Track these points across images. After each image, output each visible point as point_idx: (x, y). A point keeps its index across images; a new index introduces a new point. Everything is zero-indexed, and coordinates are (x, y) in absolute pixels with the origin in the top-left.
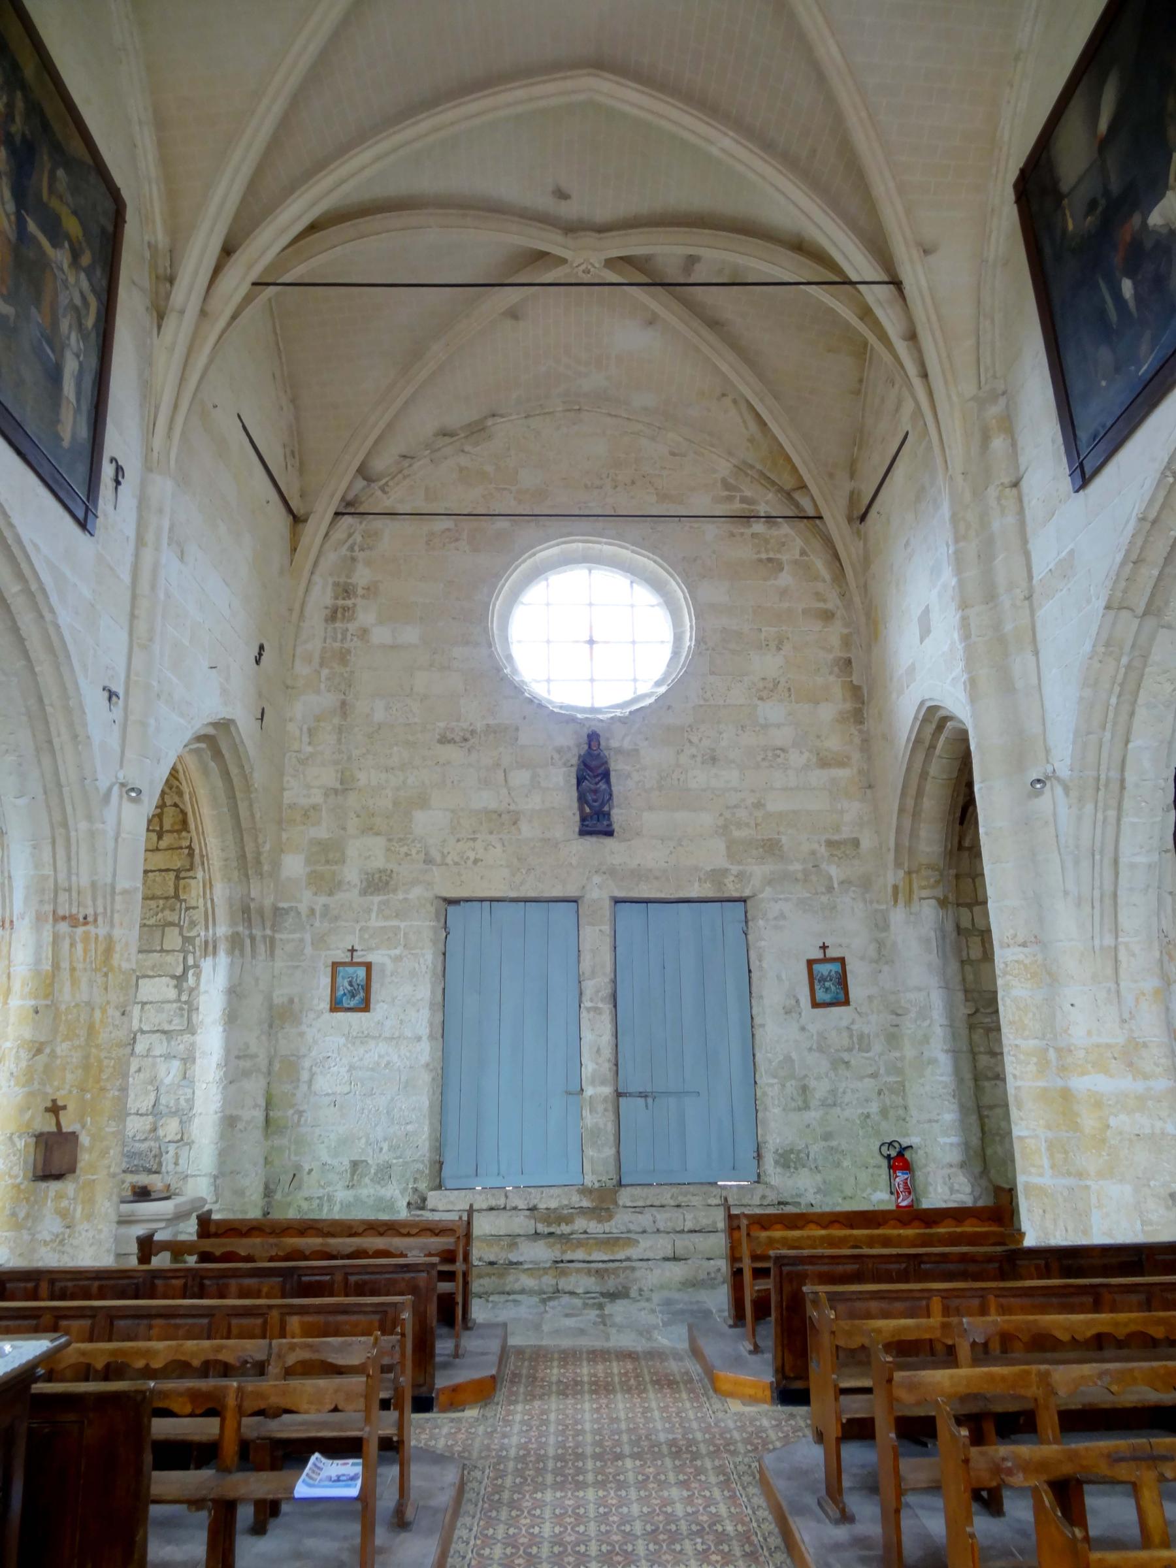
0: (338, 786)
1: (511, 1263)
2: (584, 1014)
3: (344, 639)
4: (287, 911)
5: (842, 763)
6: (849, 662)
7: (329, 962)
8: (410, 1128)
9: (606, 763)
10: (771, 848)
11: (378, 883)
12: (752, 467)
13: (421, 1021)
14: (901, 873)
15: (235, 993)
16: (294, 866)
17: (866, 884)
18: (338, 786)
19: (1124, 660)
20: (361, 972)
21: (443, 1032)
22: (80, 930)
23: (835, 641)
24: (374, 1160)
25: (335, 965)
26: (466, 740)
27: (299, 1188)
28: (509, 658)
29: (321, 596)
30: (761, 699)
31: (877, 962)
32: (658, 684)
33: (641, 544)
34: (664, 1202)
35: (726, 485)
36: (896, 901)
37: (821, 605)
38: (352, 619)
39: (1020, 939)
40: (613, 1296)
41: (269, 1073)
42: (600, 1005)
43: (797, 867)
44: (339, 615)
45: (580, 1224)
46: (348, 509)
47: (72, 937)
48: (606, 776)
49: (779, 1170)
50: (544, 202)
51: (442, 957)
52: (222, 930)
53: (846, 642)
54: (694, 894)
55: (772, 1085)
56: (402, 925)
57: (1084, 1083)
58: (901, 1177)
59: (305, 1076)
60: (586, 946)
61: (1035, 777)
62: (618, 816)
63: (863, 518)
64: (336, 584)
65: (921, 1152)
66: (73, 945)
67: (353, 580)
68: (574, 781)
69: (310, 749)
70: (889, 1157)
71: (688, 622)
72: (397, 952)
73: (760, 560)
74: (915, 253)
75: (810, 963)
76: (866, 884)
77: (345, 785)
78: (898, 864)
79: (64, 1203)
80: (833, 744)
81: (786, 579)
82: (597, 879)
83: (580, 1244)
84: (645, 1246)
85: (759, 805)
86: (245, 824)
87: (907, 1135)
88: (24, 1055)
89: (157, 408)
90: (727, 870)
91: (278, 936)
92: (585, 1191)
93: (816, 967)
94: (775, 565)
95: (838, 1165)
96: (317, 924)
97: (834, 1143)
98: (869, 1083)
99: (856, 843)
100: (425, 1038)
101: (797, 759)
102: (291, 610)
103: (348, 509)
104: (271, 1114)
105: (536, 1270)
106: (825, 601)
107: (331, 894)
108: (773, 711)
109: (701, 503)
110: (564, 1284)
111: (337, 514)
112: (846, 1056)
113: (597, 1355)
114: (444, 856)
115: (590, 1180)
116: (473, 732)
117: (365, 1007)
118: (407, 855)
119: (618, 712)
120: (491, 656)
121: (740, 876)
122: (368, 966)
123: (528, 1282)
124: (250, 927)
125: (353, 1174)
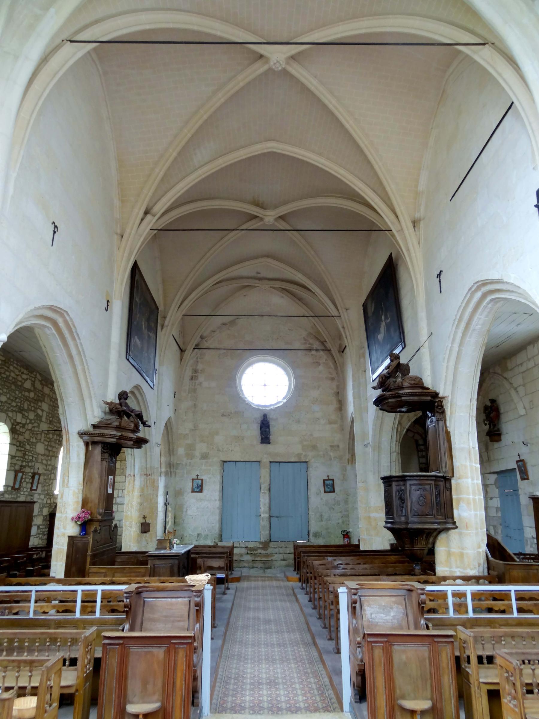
0: (193, 428)
1: (241, 561)
2: (261, 494)
3: (195, 385)
4: (179, 464)
5: (335, 422)
6: (338, 393)
7: (191, 479)
8: (213, 525)
9: (269, 423)
10: (314, 447)
11: (205, 456)
12: (312, 334)
13: (217, 495)
14: (350, 456)
15: (166, 487)
16: (181, 451)
17: (341, 458)
18: (193, 428)
19: (380, 421)
20: (200, 482)
21: (222, 498)
22: (148, 477)
23: (335, 387)
24: (203, 534)
25: (193, 480)
26: (229, 415)
27: (183, 541)
28: (242, 390)
29: (189, 373)
30: (313, 404)
31: (343, 480)
32: (284, 398)
33: (279, 357)
34: (282, 546)
35: (305, 340)
36: (348, 463)
37: (331, 376)
38: (197, 380)
39: (362, 481)
40: (267, 568)
41: (175, 509)
42: (266, 492)
43: (321, 453)
44: (194, 378)
45: (259, 551)
46: (197, 347)
47: (147, 479)
48: (268, 427)
49: (314, 538)
50: (253, 274)
51: (222, 478)
52: (163, 470)
53: (338, 387)
54: (292, 460)
55: (312, 514)
56: (212, 468)
57: (372, 515)
58: (346, 540)
59: (185, 510)
60: (262, 475)
61: (365, 444)
62: (272, 437)
63: (343, 352)
64: (193, 369)
65: (352, 533)
66: (147, 481)
67: (198, 368)
68: (259, 428)
69: (185, 418)
70: (344, 535)
71: (293, 381)
72: (210, 476)
73: (314, 362)
74: (344, 310)
75: (324, 481)
76: (341, 458)
77: (195, 428)
78: (349, 453)
79: (147, 538)
80: (333, 417)
81: (321, 368)
82: (265, 456)
83: (259, 556)
84: (276, 557)
85: (311, 435)
86: (170, 441)
87: (349, 529)
88: (139, 506)
89: (162, 349)
90: (302, 454)
91: (177, 471)
92: (261, 543)
93: (326, 482)
94: (318, 364)
95: (330, 537)
96: (188, 468)
97: (329, 531)
98: (339, 514)
99: (338, 446)
100: (218, 500)
101: (322, 422)
102: (180, 377)
103: (197, 347)
104: (176, 520)
105: (248, 562)
106: (332, 375)
107: (191, 459)
108: (316, 408)
109: (297, 345)
110: (254, 565)
111: (194, 349)
112: (333, 507)
113: (262, 577)
114: (223, 449)
115: (262, 540)
116: (231, 413)
117: (201, 491)
118: (213, 448)
119: (272, 408)
120: (237, 391)
121: (305, 456)
122: (202, 480)
123: (246, 565)
124: (170, 467)
125: (198, 537)
